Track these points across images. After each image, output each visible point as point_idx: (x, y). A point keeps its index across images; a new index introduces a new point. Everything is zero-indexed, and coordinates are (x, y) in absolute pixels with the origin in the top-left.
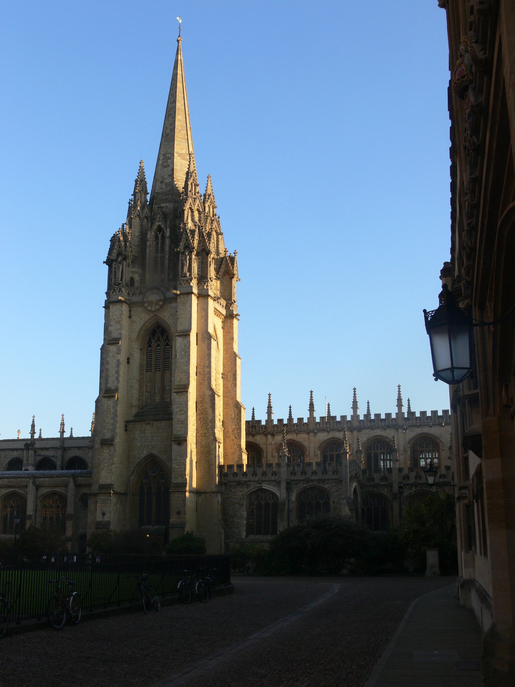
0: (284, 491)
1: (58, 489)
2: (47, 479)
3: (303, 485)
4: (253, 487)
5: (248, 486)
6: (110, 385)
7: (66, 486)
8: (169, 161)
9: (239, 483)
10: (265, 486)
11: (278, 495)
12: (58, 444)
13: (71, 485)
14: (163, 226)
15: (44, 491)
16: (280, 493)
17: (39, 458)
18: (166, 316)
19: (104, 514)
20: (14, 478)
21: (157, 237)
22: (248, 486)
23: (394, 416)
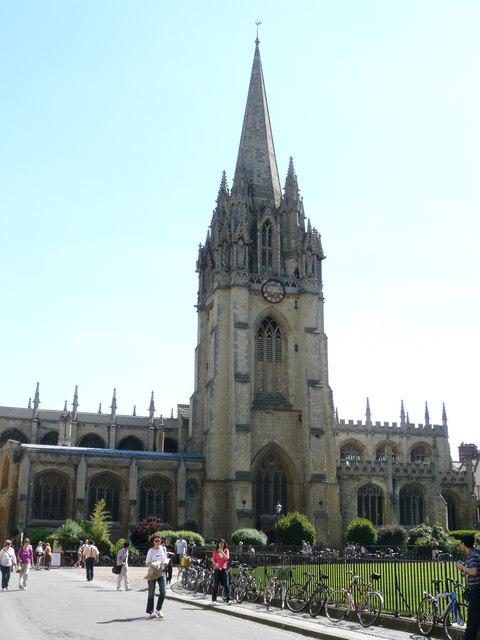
0: (391, 486)
1: (162, 473)
2: (149, 461)
3: (404, 482)
4: (364, 481)
5: (359, 480)
6: (239, 370)
7: (175, 470)
8: (264, 157)
9: (351, 476)
10: (375, 481)
11: (385, 488)
12: (108, 420)
13: (182, 470)
14: (272, 220)
15: (146, 474)
16: (385, 487)
17: (44, 432)
18: (285, 309)
19: (244, 502)
20: (109, 457)
21: (264, 230)
22: (359, 480)
23: (399, 425)
